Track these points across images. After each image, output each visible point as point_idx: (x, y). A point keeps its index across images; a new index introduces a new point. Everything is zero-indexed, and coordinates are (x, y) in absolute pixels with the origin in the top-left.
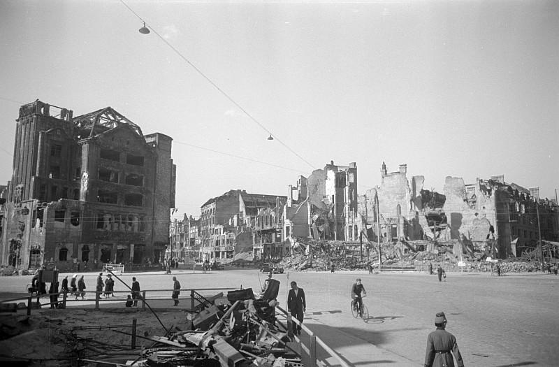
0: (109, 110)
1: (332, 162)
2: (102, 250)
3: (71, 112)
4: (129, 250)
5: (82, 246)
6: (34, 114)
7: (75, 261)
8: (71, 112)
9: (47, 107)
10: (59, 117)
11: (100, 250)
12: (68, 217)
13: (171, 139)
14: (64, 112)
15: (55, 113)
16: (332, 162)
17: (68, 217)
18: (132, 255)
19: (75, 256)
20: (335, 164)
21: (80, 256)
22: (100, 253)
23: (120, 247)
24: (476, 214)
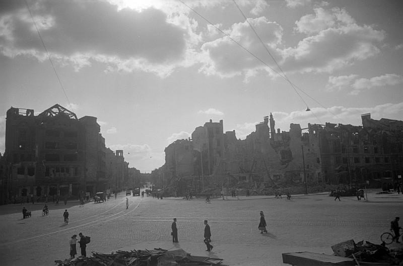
0: (57, 106)
1: (211, 120)
2: (50, 189)
3: (32, 111)
4: (69, 187)
5: (36, 187)
6: (12, 114)
7: (32, 196)
8: (32, 111)
9: (17, 110)
10: (25, 115)
11: (48, 189)
12: (26, 171)
13: (96, 118)
14: (28, 111)
15: (23, 112)
16: (211, 120)
17: (26, 171)
18: (71, 190)
19: (32, 193)
20: (213, 122)
21: (35, 192)
22: (48, 191)
23: (63, 186)
24: (309, 150)
